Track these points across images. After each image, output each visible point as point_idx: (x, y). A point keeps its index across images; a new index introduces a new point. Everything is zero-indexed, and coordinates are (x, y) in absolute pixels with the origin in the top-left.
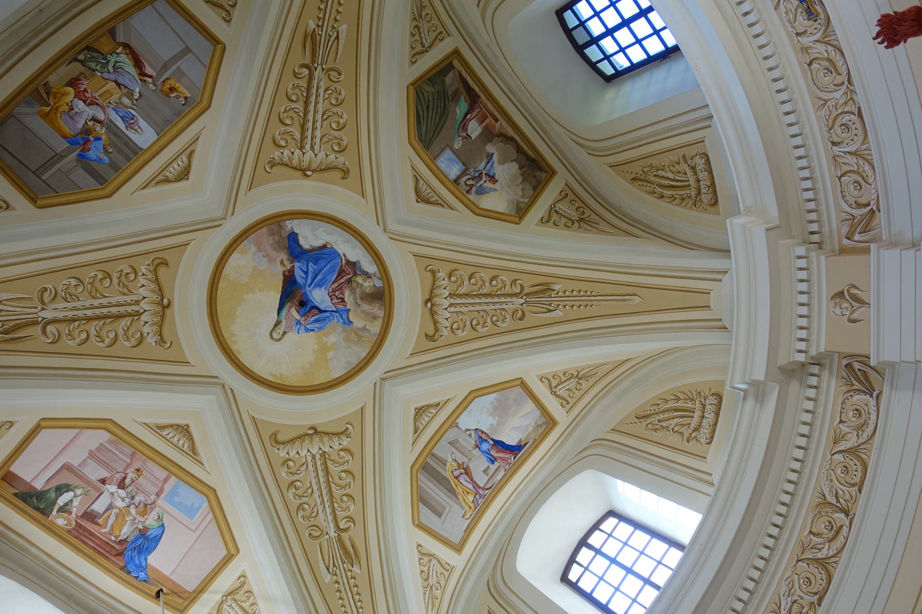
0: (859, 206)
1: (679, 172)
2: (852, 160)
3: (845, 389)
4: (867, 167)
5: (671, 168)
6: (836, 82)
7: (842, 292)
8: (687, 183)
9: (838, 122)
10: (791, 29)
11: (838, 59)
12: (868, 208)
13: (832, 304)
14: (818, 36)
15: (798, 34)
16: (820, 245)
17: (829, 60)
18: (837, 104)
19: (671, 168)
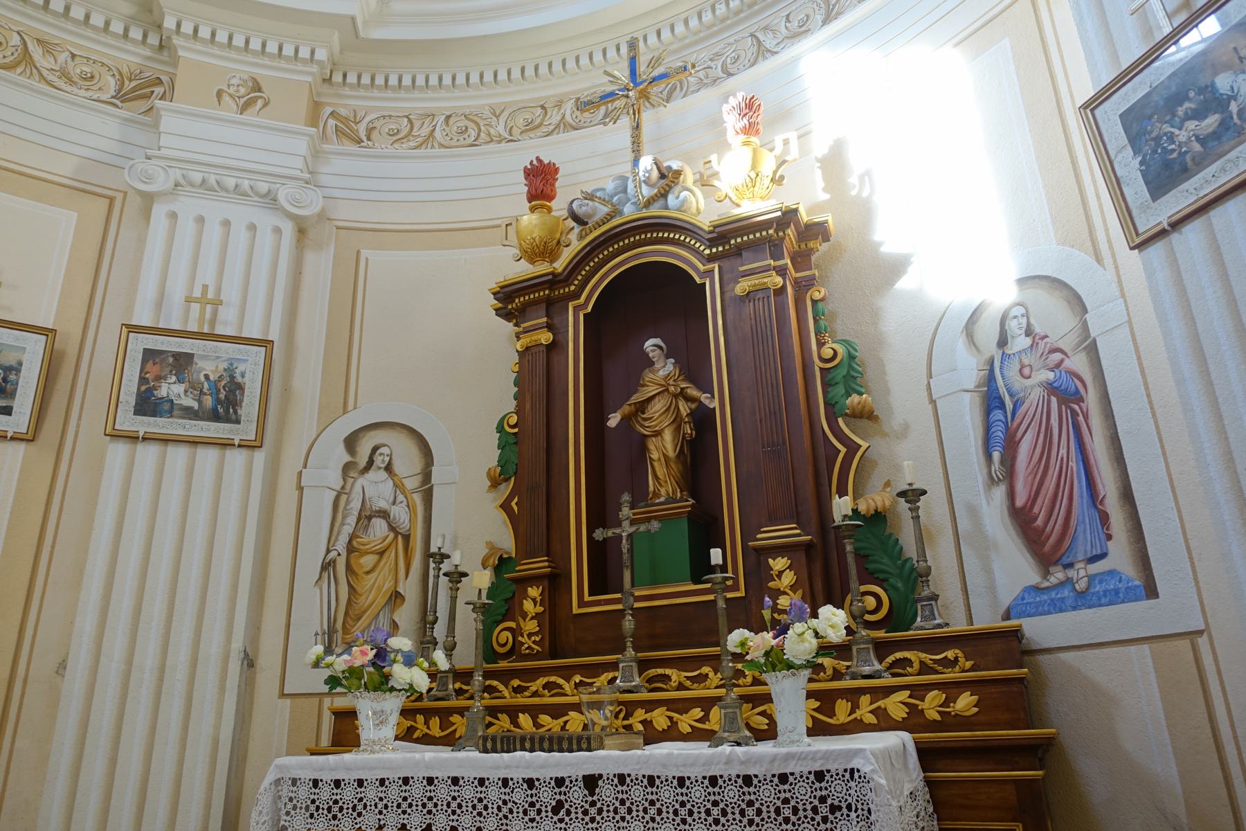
0: (369, 131)
2: (425, 131)
3: (125, 70)
4: (412, 144)
7: (260, 90)
9: (470, 125)
12: (364, 139)
13: (246, 77)
14: (568, 118)
16: (328, 80)
17: (540, 125)
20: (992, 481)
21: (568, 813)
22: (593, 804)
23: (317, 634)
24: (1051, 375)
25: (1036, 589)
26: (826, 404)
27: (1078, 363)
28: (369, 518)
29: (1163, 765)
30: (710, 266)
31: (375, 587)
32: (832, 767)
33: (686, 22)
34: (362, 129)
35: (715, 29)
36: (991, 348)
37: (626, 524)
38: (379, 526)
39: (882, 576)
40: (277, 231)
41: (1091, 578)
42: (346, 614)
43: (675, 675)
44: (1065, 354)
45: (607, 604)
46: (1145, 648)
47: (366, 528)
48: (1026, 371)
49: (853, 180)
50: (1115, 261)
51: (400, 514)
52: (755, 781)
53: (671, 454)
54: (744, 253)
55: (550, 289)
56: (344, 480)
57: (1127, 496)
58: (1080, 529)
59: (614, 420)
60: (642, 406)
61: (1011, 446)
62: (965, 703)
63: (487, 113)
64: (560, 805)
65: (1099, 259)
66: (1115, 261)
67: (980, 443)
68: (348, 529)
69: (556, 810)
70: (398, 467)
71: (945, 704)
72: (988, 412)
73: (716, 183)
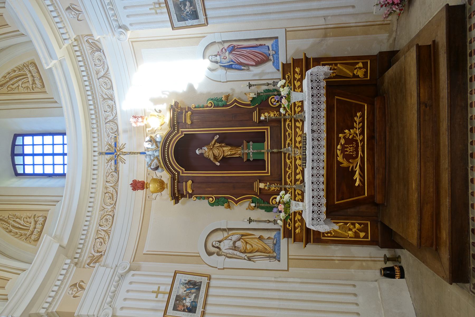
0: (98, 252)
1: (28, 222)
2: (103, 233)
4: (107, 237)
5: (25, 219)
7: (76, 284)
8: (28, 228)
9: (105, 218)
13: (70, 289)
15: (107, 181)
16: (76, 264)
17: (112, 194)
19: (25, 219)
20: (248, 70)
22: (317, 131)
24: (227, 52)
25: (273, 63)
27: (226, 45)
28: (235, 247)
29: (310, 41)
30: (180, 132)
31: (257, 244)
33: (94, 142)
34: (96, 254)
36: (217, 65)
37: (249, 151)
38: (238, 244)
40: (133, 275)
41: (273, 50)
42: (264, 253)
43: (288, 141)
47: (238, 248)
48: (225, 58)
49: (163, 96)
51: (234, 238)
53: (230, 148)
59: (218, 164)
60: (215, 157)
62: (297, 70)
63: (102, 212)
64: (317, 140)
65: (204, 37)
68: (238, 253)
69: (319, 141)
70: (220, 239)
71: (298, 74)
72: (232, 68)
73: (155, 129)
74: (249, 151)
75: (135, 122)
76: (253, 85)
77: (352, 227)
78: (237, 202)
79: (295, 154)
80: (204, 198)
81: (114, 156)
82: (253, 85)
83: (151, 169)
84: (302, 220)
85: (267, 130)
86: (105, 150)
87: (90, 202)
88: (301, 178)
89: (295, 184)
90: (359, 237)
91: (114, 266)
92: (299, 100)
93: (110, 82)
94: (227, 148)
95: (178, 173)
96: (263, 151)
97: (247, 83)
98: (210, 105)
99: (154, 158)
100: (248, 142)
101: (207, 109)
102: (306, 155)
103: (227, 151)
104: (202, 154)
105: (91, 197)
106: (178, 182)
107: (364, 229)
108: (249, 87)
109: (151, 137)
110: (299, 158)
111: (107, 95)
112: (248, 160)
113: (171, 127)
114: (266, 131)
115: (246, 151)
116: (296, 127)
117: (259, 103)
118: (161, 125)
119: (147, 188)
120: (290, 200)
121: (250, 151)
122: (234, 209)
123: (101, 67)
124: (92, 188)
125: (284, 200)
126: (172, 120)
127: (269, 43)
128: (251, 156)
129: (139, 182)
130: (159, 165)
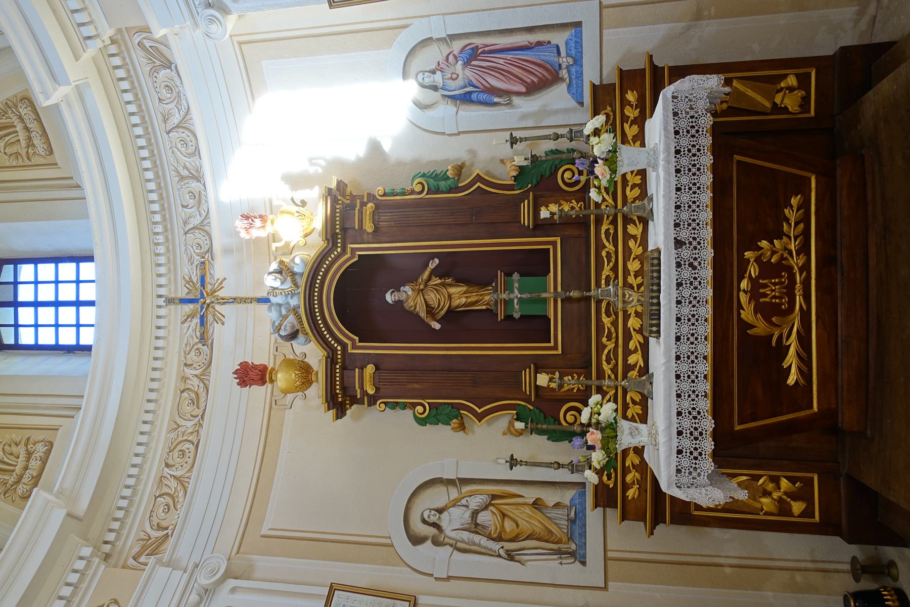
0: (160, 528)
1: (11, 454)
2: (173, 483)
4: (181, 494)
5: (7, 447)
6: (194, 413)
8: (12, 468)
9: (179, 448)
10: (183, 359)
11: (203, 395)
12: (165, 532)
15: (186, 365)
17: (197, 394)
18: (185, 431)
19: (7, 447)
20: (509, 104)
21: (695, 259)
22: (690, 243)
23: (561, 564)
24: (460, 62)
25: (569, 86)
26: (449, 193)
27: (457, 46)
28: (477, 525)
30: (349, 250)
31: (529, 520)
32: (671, 108)
33: (160, 275)
34: (155, 534)
35: (171, 257)
36: (437, 95)
37: (512, 296)
38: (483, 517)
39: (553, 168)
40: (233, 590)
41: (568, 55)
42: (547, 541)
43: (606, 271)
44: (449, 54)
45: (557, 331)
46: (604, 32)
47: (484, 527)
48: (454, 76)
49: (312, 170)
50: (410, 18)
51: (475, 502)
52: (678, 148)
53: (464, 289)
54: (346, 226)
55: (336, 364)
56: (445, 545)
57: (530, 30)
58: (543, 58)
59: (437, 326)
60: (430, 310)
61: (493, 91)
62: (631, 97)
64: (691, 265)
66: (410, 18)
67: (487, 108)
68: (484, 541)
69: (694, 268)
70: (440, 504)
71: (632, 106)
72: (471, 102)
73: (292, 245)
74: (512, 296)
75: (247, 229)
76: (521, 140)
77: (770, 486)
78: (480, 417)
79: (624, 302)
80: (404, 406)
81: (198, 306)
82: (521, 140)
83: (281, 336)
84: (643, 467)
85: (554, 245)
86: (182, 293)
87: (147, 412)
88: (641, 363)
89: (625, 377)
90: (789, 513)
91: (191, 565)
92: (636, 168)
93: (193, 139)
94: (459, 289)
95: (344, 346)
96: (544, 295)
97: (507, 135)
98: (418, 188)
99: (289, 311)
100: (509, 274)
101: (413, 197)
102: (659, 304)
103: (460, 296)
104: (399, 303)
105: (149, 401)
106: (344, 368)
107: (804, 494)
108: (512, 144)
109: (281, 262)
110: (636, 312)
111: (187, 169)
112: (509, 318)
113: (327, 239)
114: (551, 247)
115: (504, 296)
116: (627, 236)
117: (535, 182)
118: (306, 236)
119: (272, 381)
120: (615, 419)
121: (513, 295)
122: (473, 432)
123: (172, 105)
124: (153, 380)
125: (600, 418)
126: (330, 222)
127: (559, 39)
128: (517, 307)
129: (255, 367)
130: (298, 327)
